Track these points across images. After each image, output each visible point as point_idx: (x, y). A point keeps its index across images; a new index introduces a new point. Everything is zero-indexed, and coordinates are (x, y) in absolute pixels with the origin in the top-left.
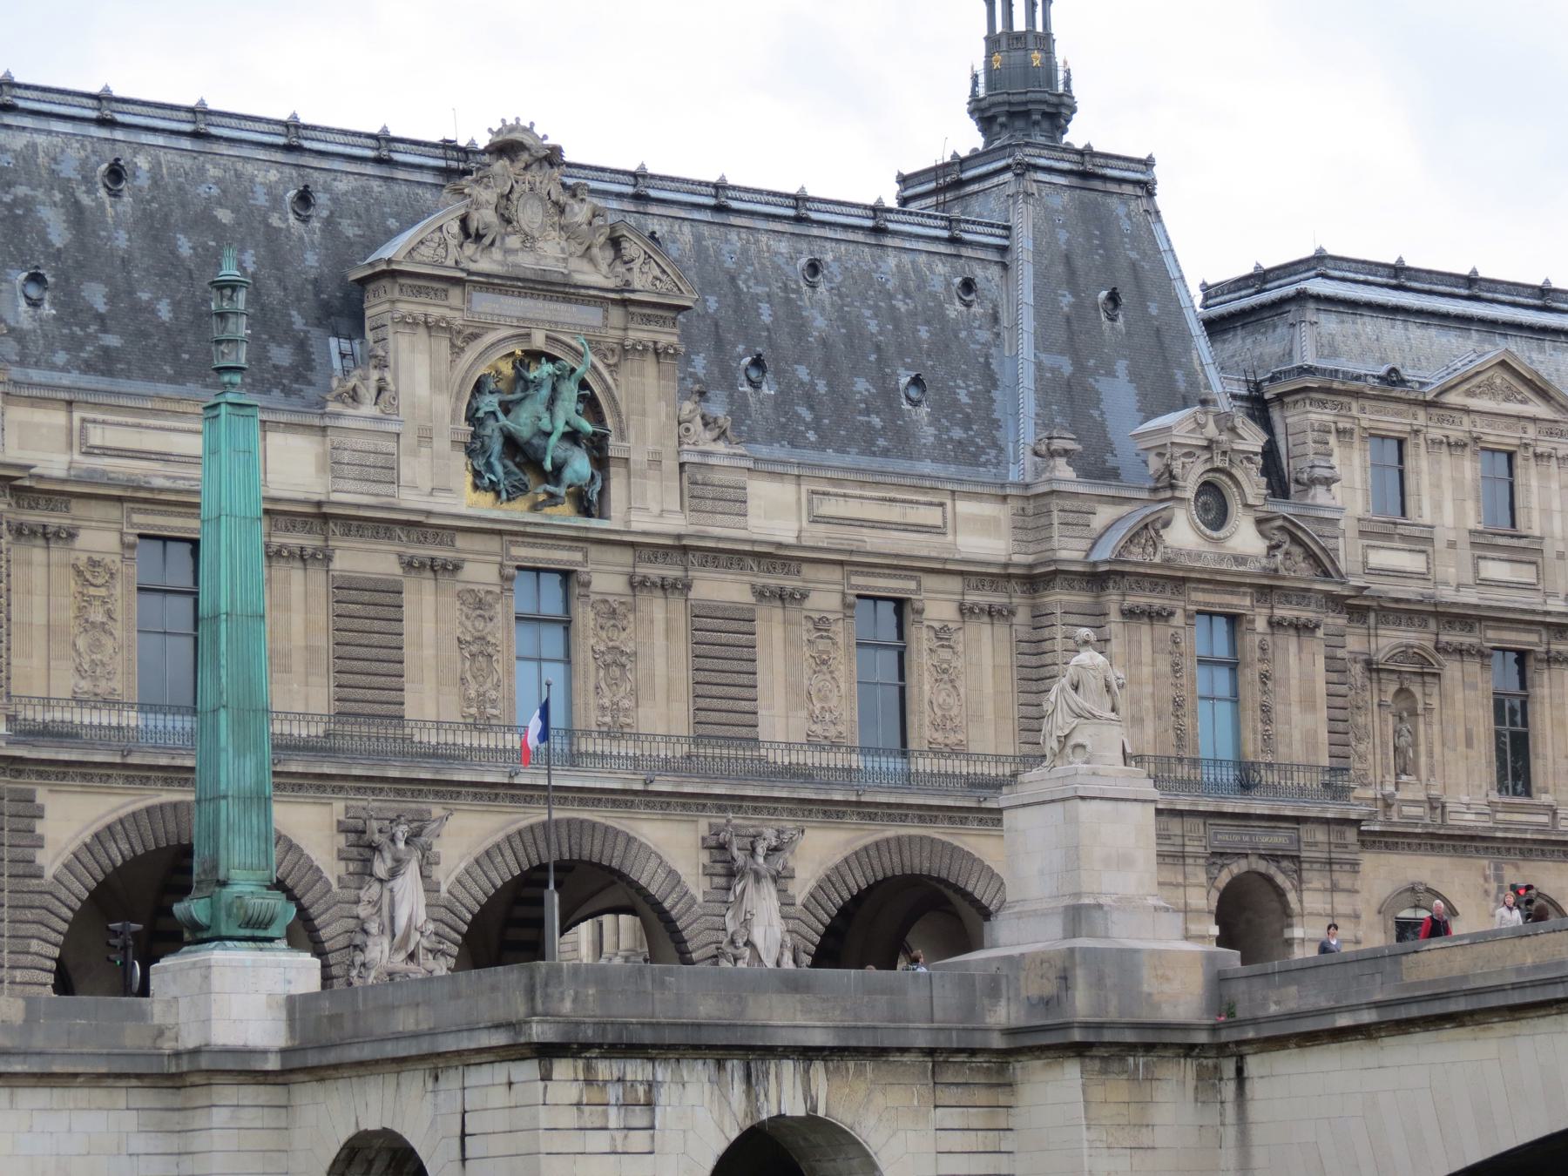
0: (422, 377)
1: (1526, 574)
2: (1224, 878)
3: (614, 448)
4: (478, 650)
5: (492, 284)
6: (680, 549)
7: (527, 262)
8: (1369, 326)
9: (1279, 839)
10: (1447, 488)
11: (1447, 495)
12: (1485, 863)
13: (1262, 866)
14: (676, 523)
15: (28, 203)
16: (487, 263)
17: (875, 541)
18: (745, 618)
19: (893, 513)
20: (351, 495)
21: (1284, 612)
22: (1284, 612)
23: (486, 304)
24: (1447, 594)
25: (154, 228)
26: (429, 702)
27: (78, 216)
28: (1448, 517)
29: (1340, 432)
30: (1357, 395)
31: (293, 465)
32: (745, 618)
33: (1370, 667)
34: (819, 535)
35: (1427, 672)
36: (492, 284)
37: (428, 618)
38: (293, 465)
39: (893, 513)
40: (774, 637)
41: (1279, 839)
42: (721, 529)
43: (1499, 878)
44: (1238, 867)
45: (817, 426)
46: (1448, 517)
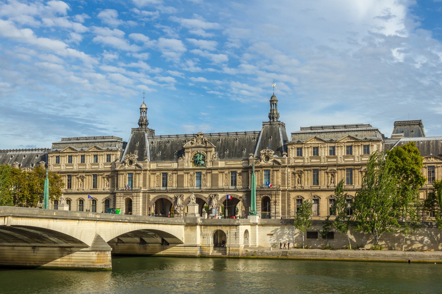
0: (188, 156)
1: (319, 160)
2: (262, 197)
3: (206, 160)
4: (191, 180)
5: (193, 147)
6: (210, 169)
7: (198, 145)
8: (300, 135)
9: (269, 192)
10: (307, 152)
11: (307, 153)
12: (310, 193)
13: (266, 195)
14: (211, 167)
15: (161, 146)
16: (193, 146)
17: (233, 166)
18: (217, 175)
19: (235, 163)
20: (180, 167)
21: (274, 169)
22: (274, 169)
23: (193, 149)
24: (305, 164)
25: (172, 146)
26: (186, 185)
27: (165, 146)
28: (307, 155)
29: (292, 148)
30: (294, 144)
31: (175, 165)
32: (217, 175)
33: (294, 173)
34: (227, 166)
35: (301, 172)
36: (193, 147)
37: (186, 178)
38: (175, 165)
39: (235, 163)
40: (220, 176)
41: (269, 192)
42: (215, 166)
43: (311, 194)
44: (264, 196)
45: (232, 155)
46: (307, 155)
